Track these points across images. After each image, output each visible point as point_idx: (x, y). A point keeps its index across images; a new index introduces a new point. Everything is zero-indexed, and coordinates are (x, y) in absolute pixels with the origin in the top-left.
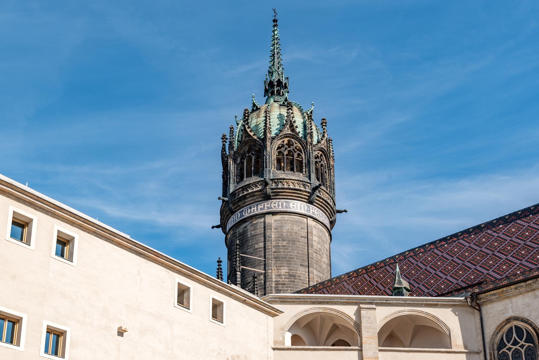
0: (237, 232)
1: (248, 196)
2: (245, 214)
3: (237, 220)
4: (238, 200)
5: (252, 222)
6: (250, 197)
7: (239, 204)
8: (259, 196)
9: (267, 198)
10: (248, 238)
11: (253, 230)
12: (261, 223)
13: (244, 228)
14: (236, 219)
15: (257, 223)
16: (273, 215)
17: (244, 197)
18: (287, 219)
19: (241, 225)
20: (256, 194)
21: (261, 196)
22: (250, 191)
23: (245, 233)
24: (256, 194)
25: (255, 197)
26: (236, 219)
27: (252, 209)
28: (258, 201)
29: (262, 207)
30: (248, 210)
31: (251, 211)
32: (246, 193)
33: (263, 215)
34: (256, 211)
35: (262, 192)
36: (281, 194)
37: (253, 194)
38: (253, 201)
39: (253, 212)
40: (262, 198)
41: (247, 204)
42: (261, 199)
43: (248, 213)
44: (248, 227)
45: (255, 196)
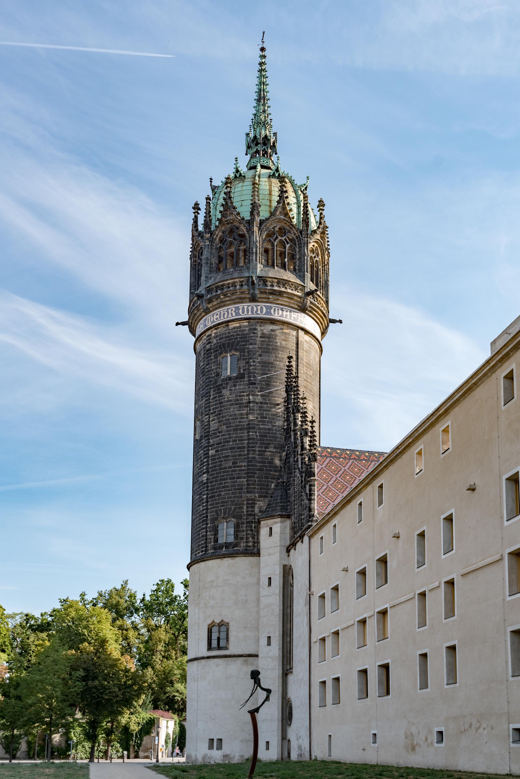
0: (259, 330)
1: (285, 295)
2: (275, 314)
3: (259, 314)
4: (271, 291)
5: (283, 329)
6: (287, 297)
7: (270, 297)
8: (296, 303)
9: (303, 309)
10: (277, 346)
11: (283, 340)
12: (293, 335)
13: (271, 330)
14: (259, 312)
15: (289, 334)
16: (305, 333)
17: (280, 294)
18: (313, 345)
19: (265, 323)
20: (295, 298)
21: (298, 303)
22: (289, 291)
23: (273, 338)
24: (295, 298)
25: (292, 302)
26: (259, 312)
27: (285, 313)
28: (292, 307)
29: (295, 316)
30: (278, 310)
31: (282, 313)
32: (283, 289)
33: (298, 328)
34: (288, 317)
35: (302, 301)
36: (315, 313)
37: (291, 296)
38: (287, 304)
39: (285, 318)
40: (299, 306)
41: (279, 302)
42: (296, 307)
43: (278, 314)
44: (278, 332)
45: (292, 299)
